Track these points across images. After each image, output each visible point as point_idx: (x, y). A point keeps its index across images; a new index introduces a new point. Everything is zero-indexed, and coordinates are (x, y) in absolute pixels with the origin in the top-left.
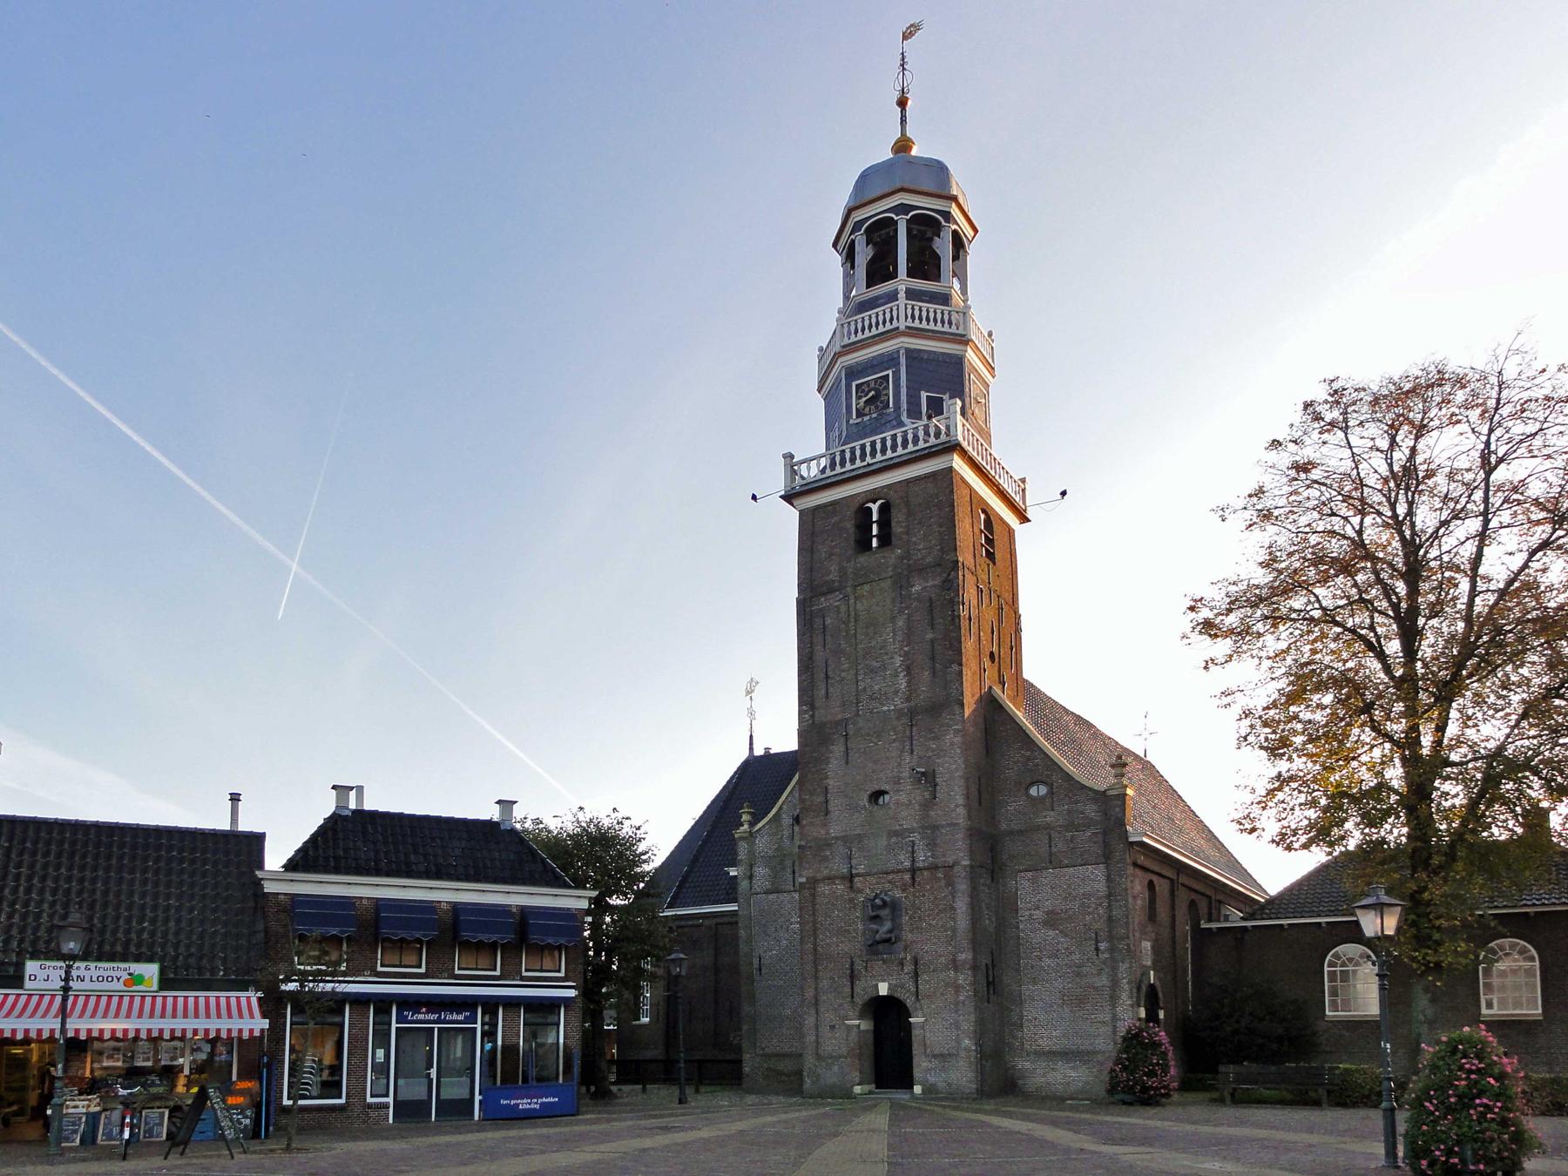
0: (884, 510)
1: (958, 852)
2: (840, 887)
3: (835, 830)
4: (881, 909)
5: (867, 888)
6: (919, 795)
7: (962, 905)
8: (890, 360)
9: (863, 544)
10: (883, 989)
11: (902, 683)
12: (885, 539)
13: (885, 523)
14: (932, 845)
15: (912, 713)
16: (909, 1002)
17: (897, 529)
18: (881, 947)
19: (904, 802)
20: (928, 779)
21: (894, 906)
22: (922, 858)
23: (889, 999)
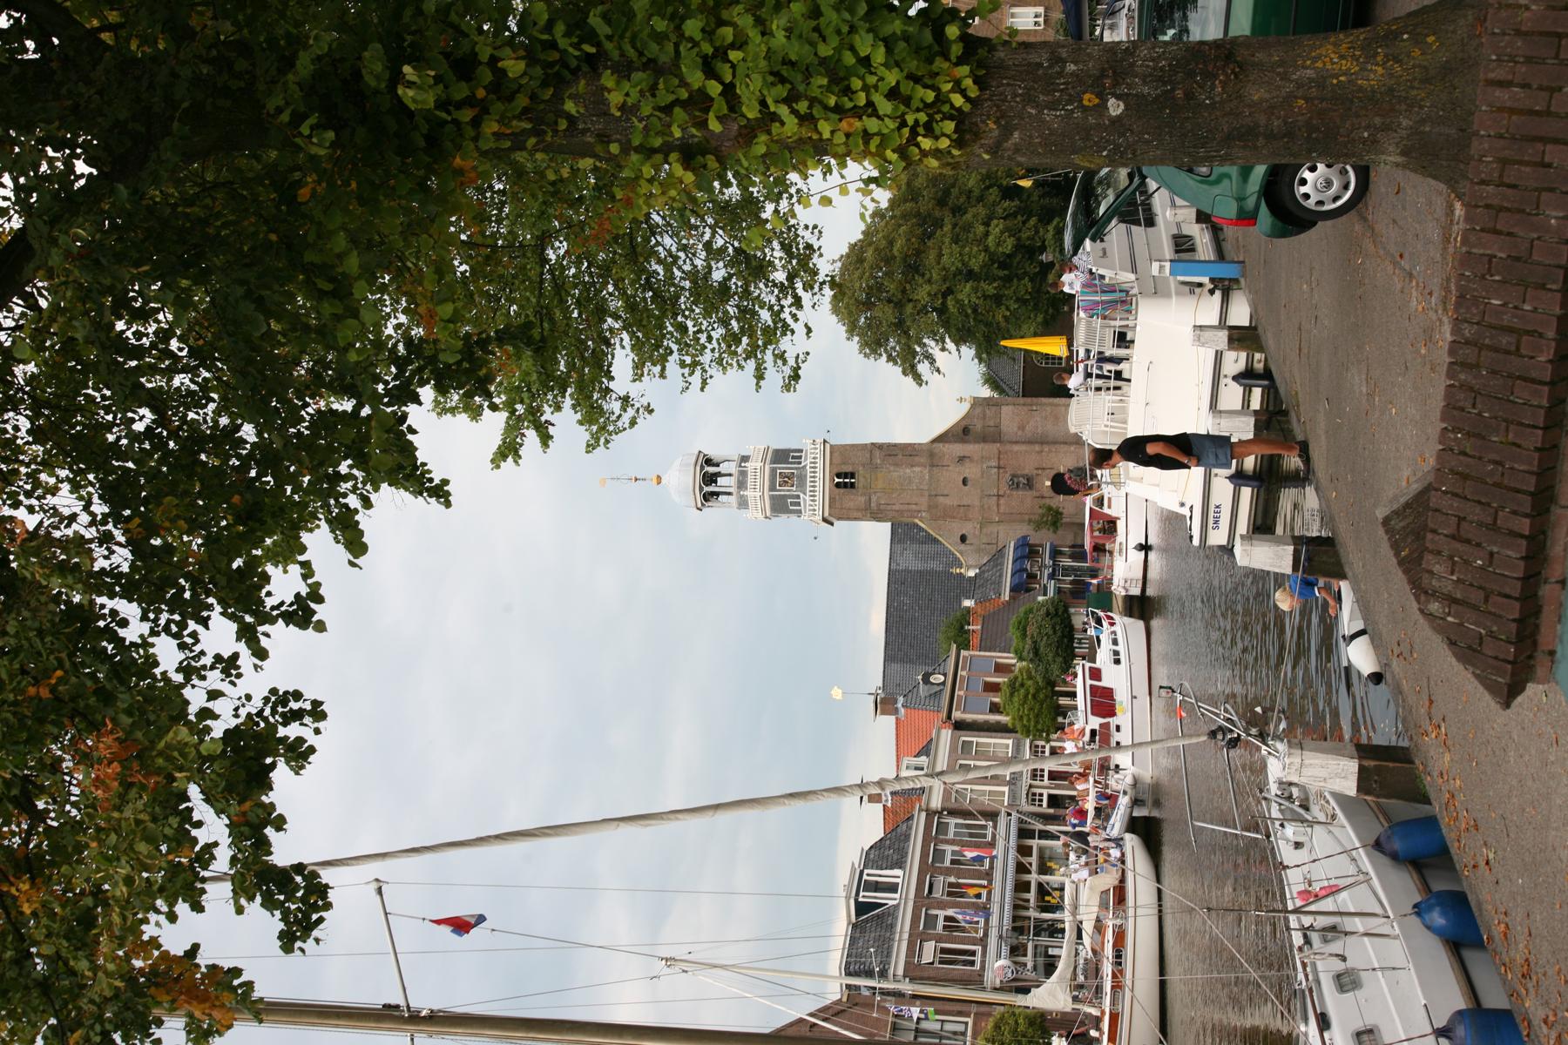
0: (838, 476)
1: (993, 448)
2: (1002, 501)
3: (977, 503)
4: (1015, 484)
5: (1004, 489)
6: (967, 464)
7: (1016, 448)
8: (773, 471)
9: (852, 485)
10: (1048, 483)
11: (917, 469)
12: (852, 475)
13: (846, 475)
14: (989, 459)
15: (932, 466)
16: (1053, 473)
17: (848, 469)
18: (1030, 483)
19: (970, 471)
20: (961, 459)
21: (1014, 476)
22: (994, 464)
23: (1053, 482)
